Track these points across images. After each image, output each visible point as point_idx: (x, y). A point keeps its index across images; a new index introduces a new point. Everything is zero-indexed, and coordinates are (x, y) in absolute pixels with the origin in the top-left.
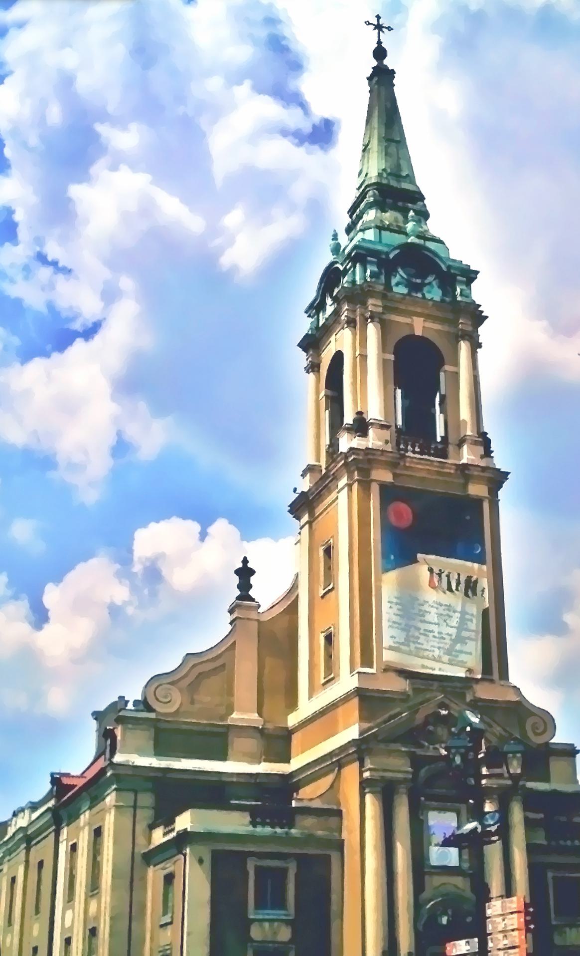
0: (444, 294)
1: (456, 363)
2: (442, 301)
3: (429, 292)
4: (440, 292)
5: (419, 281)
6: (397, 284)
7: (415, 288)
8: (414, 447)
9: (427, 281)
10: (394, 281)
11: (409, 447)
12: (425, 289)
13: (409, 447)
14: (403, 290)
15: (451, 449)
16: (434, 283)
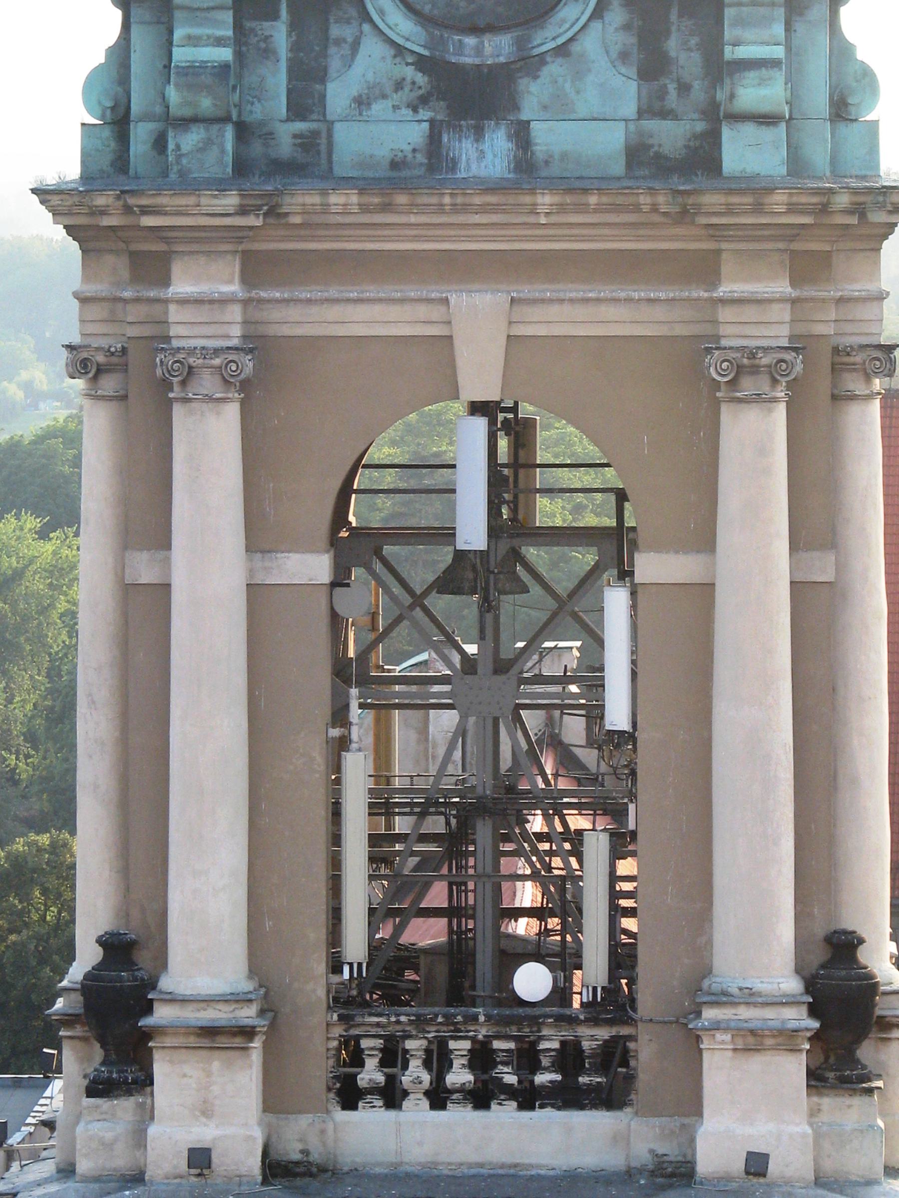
0: (653, 108)
1: (704, 539)
2: (637, 154)
3: (559, 108)
4: (627, 93)
5: (497, 48)
6: (361, 102)
7: (468, 97)
8: (437, 1059)
9: (545, 39)
10: (338, 94)
11: (416, 1074)
12: (533, 95)
13: (416, 1074)
14: (399, 133)
15: (646, 1051)
16: (590, 44)
